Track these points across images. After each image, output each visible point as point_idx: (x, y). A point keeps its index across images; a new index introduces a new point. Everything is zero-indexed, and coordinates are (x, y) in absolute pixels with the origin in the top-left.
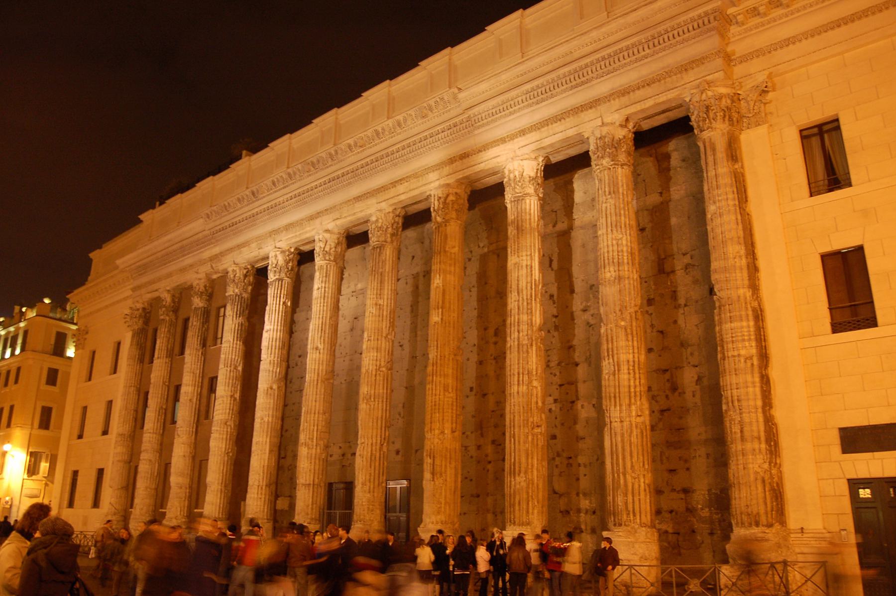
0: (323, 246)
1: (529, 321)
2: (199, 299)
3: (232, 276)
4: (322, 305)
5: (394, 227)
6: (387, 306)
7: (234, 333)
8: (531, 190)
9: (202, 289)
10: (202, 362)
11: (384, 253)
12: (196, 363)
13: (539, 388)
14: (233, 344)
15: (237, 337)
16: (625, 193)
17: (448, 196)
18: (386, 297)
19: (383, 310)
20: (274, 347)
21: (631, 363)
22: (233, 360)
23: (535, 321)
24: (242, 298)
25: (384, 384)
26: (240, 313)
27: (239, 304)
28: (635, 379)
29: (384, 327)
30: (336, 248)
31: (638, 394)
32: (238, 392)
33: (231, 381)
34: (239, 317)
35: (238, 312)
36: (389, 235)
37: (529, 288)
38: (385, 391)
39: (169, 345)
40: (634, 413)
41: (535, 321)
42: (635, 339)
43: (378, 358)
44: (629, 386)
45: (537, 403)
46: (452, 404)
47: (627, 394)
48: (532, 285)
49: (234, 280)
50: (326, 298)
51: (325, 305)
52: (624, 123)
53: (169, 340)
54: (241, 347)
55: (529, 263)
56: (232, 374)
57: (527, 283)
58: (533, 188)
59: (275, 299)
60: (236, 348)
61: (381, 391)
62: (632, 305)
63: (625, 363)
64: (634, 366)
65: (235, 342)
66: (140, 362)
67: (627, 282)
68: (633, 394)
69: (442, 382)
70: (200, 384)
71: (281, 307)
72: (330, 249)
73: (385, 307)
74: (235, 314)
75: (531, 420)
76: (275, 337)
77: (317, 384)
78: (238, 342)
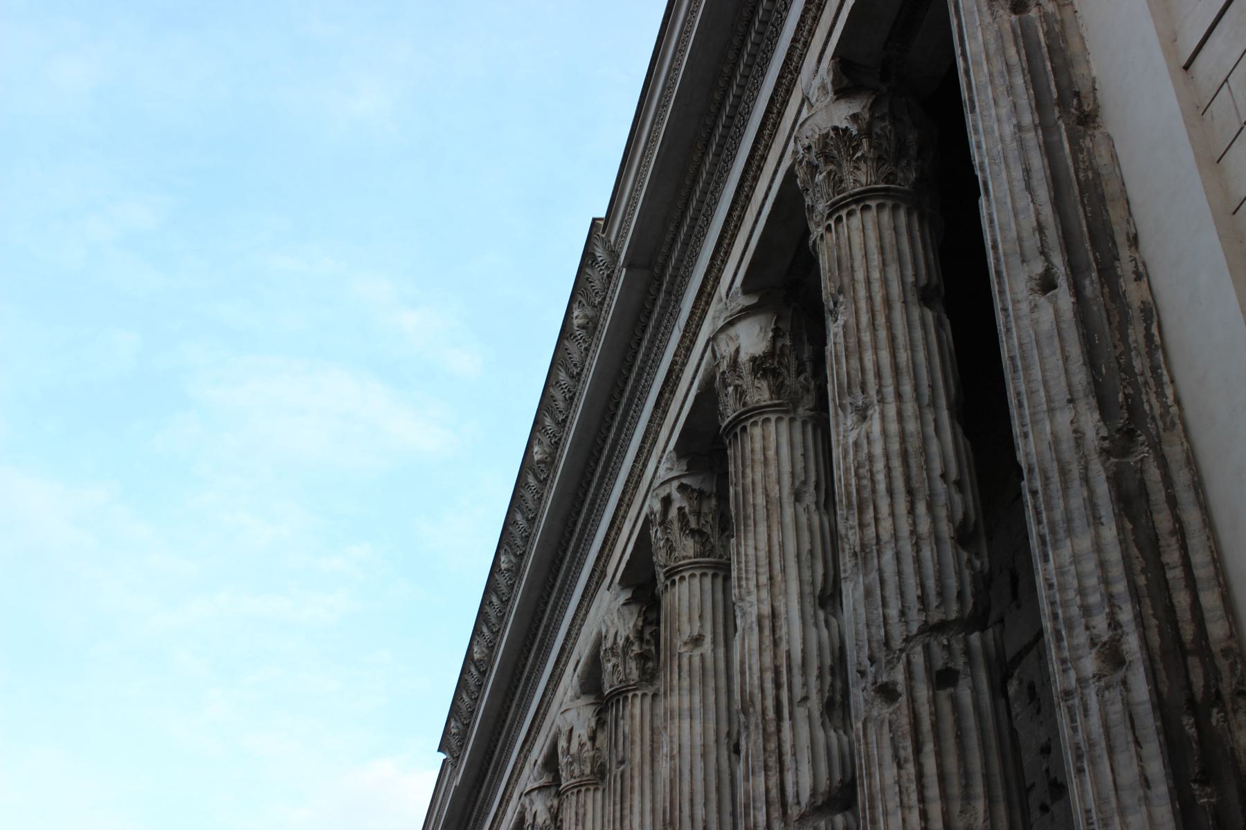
1: (774, 793)
5: (647, 636)
8: (760, 393)
11: (627, 712)
16: (876, 275)
17: (667, 501)
23: (797, 783)
30: (593, 738)
37: (769, 686)
41: (797, 783)
42: (929, 747)
52: (846, 82)
55: (766, 610)
57: (762, 671)
58: (764, 384)
62: (914, 628)
67: (888, 556)
72: (582, 745)
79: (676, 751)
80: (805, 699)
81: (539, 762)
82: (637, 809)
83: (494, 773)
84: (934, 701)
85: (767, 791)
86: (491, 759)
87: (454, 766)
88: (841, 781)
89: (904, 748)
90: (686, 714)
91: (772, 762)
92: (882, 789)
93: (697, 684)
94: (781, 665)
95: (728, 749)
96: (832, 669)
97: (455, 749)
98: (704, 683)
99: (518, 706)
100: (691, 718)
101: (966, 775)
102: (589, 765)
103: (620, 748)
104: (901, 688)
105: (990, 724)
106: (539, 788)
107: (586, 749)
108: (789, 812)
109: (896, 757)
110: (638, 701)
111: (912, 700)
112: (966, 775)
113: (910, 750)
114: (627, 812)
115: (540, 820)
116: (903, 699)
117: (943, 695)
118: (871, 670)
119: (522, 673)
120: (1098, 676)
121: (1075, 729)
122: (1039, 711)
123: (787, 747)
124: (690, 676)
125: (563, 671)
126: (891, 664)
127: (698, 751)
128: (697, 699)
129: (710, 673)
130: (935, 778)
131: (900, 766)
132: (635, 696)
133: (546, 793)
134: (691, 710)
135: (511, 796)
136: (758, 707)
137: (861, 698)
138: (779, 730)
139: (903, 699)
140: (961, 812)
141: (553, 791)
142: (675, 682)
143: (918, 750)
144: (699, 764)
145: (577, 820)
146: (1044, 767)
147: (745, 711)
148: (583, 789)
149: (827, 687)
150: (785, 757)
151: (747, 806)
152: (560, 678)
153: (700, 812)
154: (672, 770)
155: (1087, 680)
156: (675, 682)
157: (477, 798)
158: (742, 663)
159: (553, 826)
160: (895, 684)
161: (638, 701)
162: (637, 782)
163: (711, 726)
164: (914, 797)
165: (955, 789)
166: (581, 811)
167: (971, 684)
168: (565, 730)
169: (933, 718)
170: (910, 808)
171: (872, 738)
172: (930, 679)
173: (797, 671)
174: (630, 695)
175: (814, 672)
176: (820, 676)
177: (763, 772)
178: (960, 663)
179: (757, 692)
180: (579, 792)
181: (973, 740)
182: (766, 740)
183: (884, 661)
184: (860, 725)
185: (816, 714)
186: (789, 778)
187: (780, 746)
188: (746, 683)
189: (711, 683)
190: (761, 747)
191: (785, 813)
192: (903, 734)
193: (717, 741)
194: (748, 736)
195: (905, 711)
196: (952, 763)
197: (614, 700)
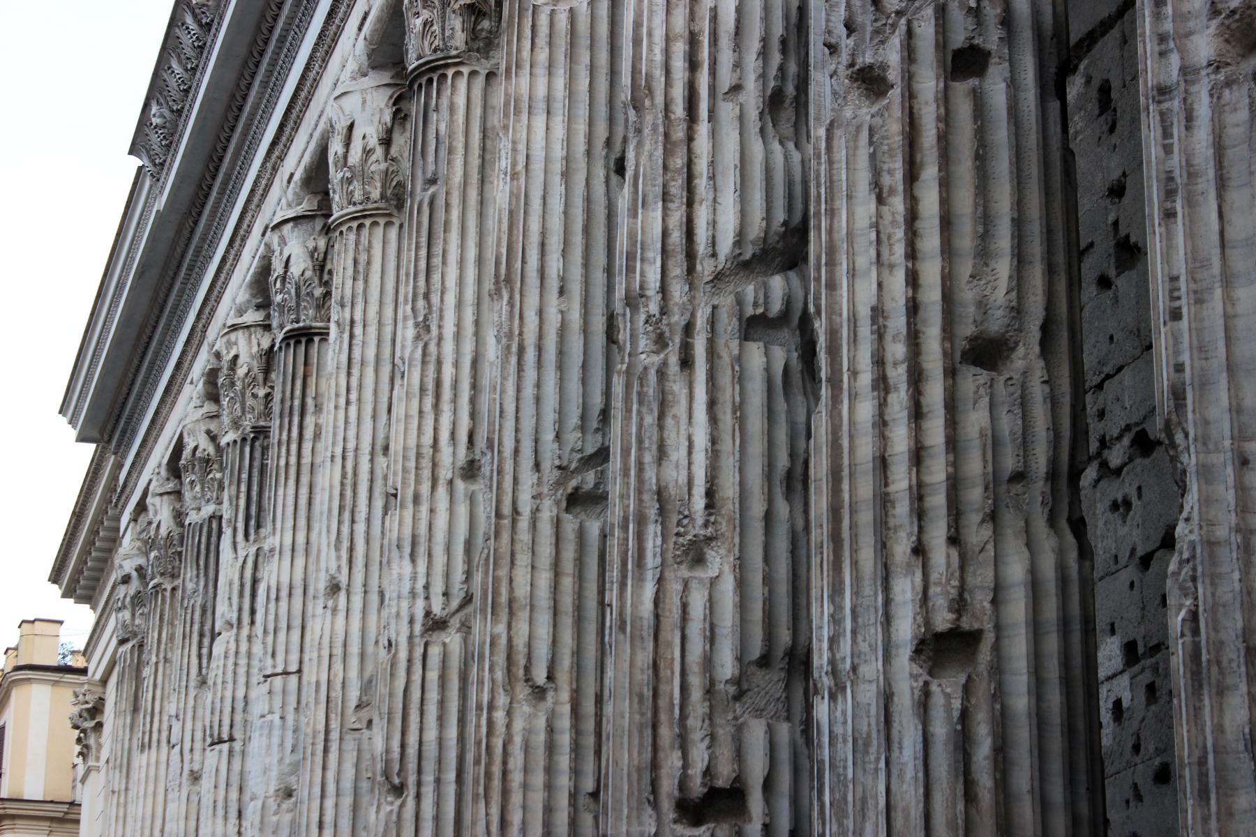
0: (341, 151)
1: (677, 237)
2: (198, 488)
4: (342, 401)
6: (458, 336)
11: (445, 101)
13: (728, 585)
14: (237, 641)
18: (451, 299)
19: (439, 363)
21: (897, 323)
23: (713, 224)
25: (442, 703)
28: (917, 413)
29: (444, 436)
30: (386, 142)
31: (938, 501)
36: (456, 23)
38: (452, 733)
40: (905, 629)
41: (713, 224)
42: (930, 172)
43: (421, 582)
44: (882, 463)
45: (708, 663)
46: (551, 748)
47: (866, 517)
48: (693, 41)
50: (356, 371)
51: (353, 396)
57: (668, 39)
60: (249, 655)
61: (431, 735)
63: (865, 331)
64: (914, 338)
65: (245, 631)
68: (902, 509)
69: (503, 641)
72: (367, 152)
73: (448, 347)
75: (671, 762)
76: (285, 580)
77: (326, 750)
79: (520, 167)
80: (736, 88)
81: (297, 177)
82: (453, 257)
83: (222, 192)
84: (945, 98)
85: (665, 233)
86: (217, 169)
87: (156, 178)
88: (785, 223)
89: (890, 172)
90: (541, 106)
91: (677, 188)
92: (850, 235)
93: (561, 58)
94: (701, 31)
95: (607, 167)
96: (784, 42)
97: (158, 150)
98: (572, 56)
99: (265, 84)
100: (548, 113)
101: (986, 219)
102: (378, 185)
103: (431, 158)
104: (893, 75)
105: (1032, 139)
106: (295, 219)
107: (373, 158)
108: (699, 268)
109: (876, 185)
110: (462, 84)
111: (910, 95)
112: (986, 219)
113: (899, 175)
114: (437, 261)
115: (295, 270)
116: (895, 94)
117: (961, 88)
118: (847, 44)
119: (271, 30)
120: (1216, 65)
121: (1168, 149)
122: (1112, 129)
123: (702, 166)
124: (550, 44)
125: (340, 29)
126: (880, 35)
127: (557, 167)
128: (560, 83)
129: (584, 42)
130: (937, 222)
131: (880, 200)
132: (458, 74)
133: (305, 226)
134: (549, 100)
135: (248, 232)
136: (659, 99)
137: (828, 90)
138: (690, 139)
139: (895, 94)
140: (972, 276)
141: (319, 224)
142: (526, 53)
143: (912, 175)
144: (557, 188)
145: (356, 271)
146: (1111, 219)
147: (637, 105)
148: (368, 222)
149: (773, 71)
150: (697, 181)
151: (631, 257)
152: (335, 40)
153: (554, 265)
154: (514, 195)
155: (1197, 71)
156: (526, 53)
157: (192, 232)
158: (637, 25)
159: (316, 281)
160: (884, 67)
161: (462, 84)
162: (455, 214)
163: (581, 128)
164: (900, 249)
165: (966, 240)
166: (363, 258)
167: (1008, 75)
168: (342, 125)
169: (941, 125)
170: (892, 267)
171: (841, 154)
172: (942, 63)
173: (725, 42)
174: (450, 72)
175: (754, 45)
176: (764, 53)
177: (660, 204)
178: (992, 39)
179: (659, 74)
180: (360, 226)
181: (1002, 165)
182: (668, 153)
183: (869, 29)
184: (822, 132)
185: (753, 114)
186: (702, 216)
187: (690, 164)
188: (641, 59)
189: (585, 58)
190: (660, 162)
191: (691, 270)
192: (890, 149)
193: (589, 153)
194: (639, 145)
195: (897, 112)
196: (965, 199)
197: (424, 80)
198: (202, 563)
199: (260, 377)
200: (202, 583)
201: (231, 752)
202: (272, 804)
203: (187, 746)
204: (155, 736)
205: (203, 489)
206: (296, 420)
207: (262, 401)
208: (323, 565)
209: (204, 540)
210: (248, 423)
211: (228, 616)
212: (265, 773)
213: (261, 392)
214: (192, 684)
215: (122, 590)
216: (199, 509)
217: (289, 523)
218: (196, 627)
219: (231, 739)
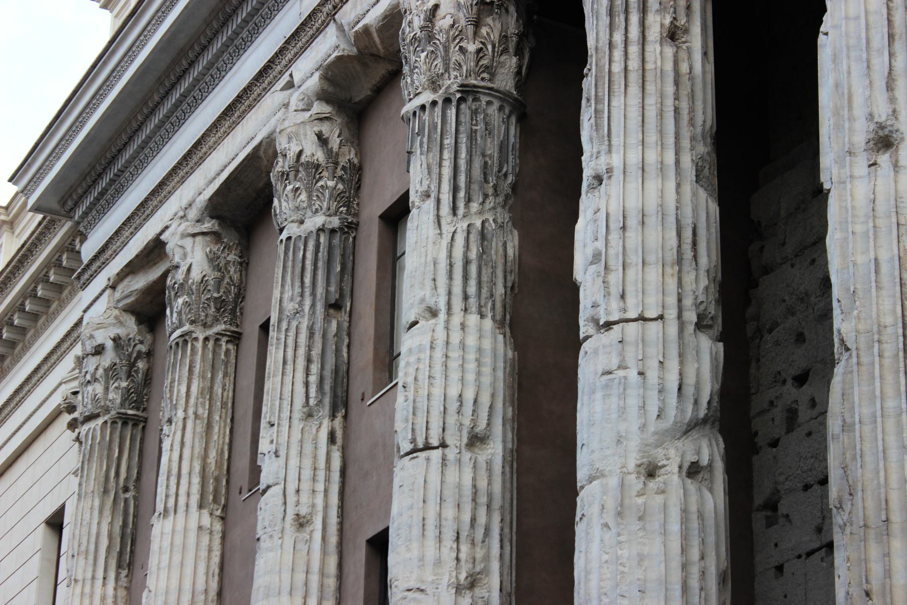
2: (303, 196)
3: (418, 22)
7: (450, 277)
9: (313, 151)
10: (336, 476)
12: (306, 486)
15: (466, 297)
20: (635, 259)
22: (453, 406)
24: (475, 113)
26: (469, 183)
27: (463, 139)
32: (495, 566)
33: (449, 512)
34: (469, 200)
35: (462, 179)
39: (213, 454)
49: (430, 38)
53: (209, 427)
54: (487, 344)
56: (452, 475)
59: (620, 20)
60: (463, 346)
65: (457, 319)
66: (119, 566)
70: (331, 582)
71: (653, 49)
74: (446, 187)
76: (633, 204)
78: (473, 319)
198: (308, 280)
199: (471, 29)
200: (308, 302)
201: (444, 459)
202: (635, 482)
203: (291, 487)
204: (182, 500)
205: (310, 197)
206: (634, 18)
207: (472, 57)
208: (860, 111)
209: (309, 255)
210: (452, 83)
211: (432, 303)
212: (619, 442)
213: (472, 47)
214: (297, 415)
215: (91, 364)
216: (302, 222)
217: (634, 137)
218: (302, 351)
219: (443, 445)
